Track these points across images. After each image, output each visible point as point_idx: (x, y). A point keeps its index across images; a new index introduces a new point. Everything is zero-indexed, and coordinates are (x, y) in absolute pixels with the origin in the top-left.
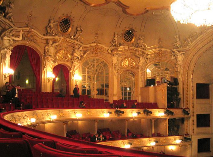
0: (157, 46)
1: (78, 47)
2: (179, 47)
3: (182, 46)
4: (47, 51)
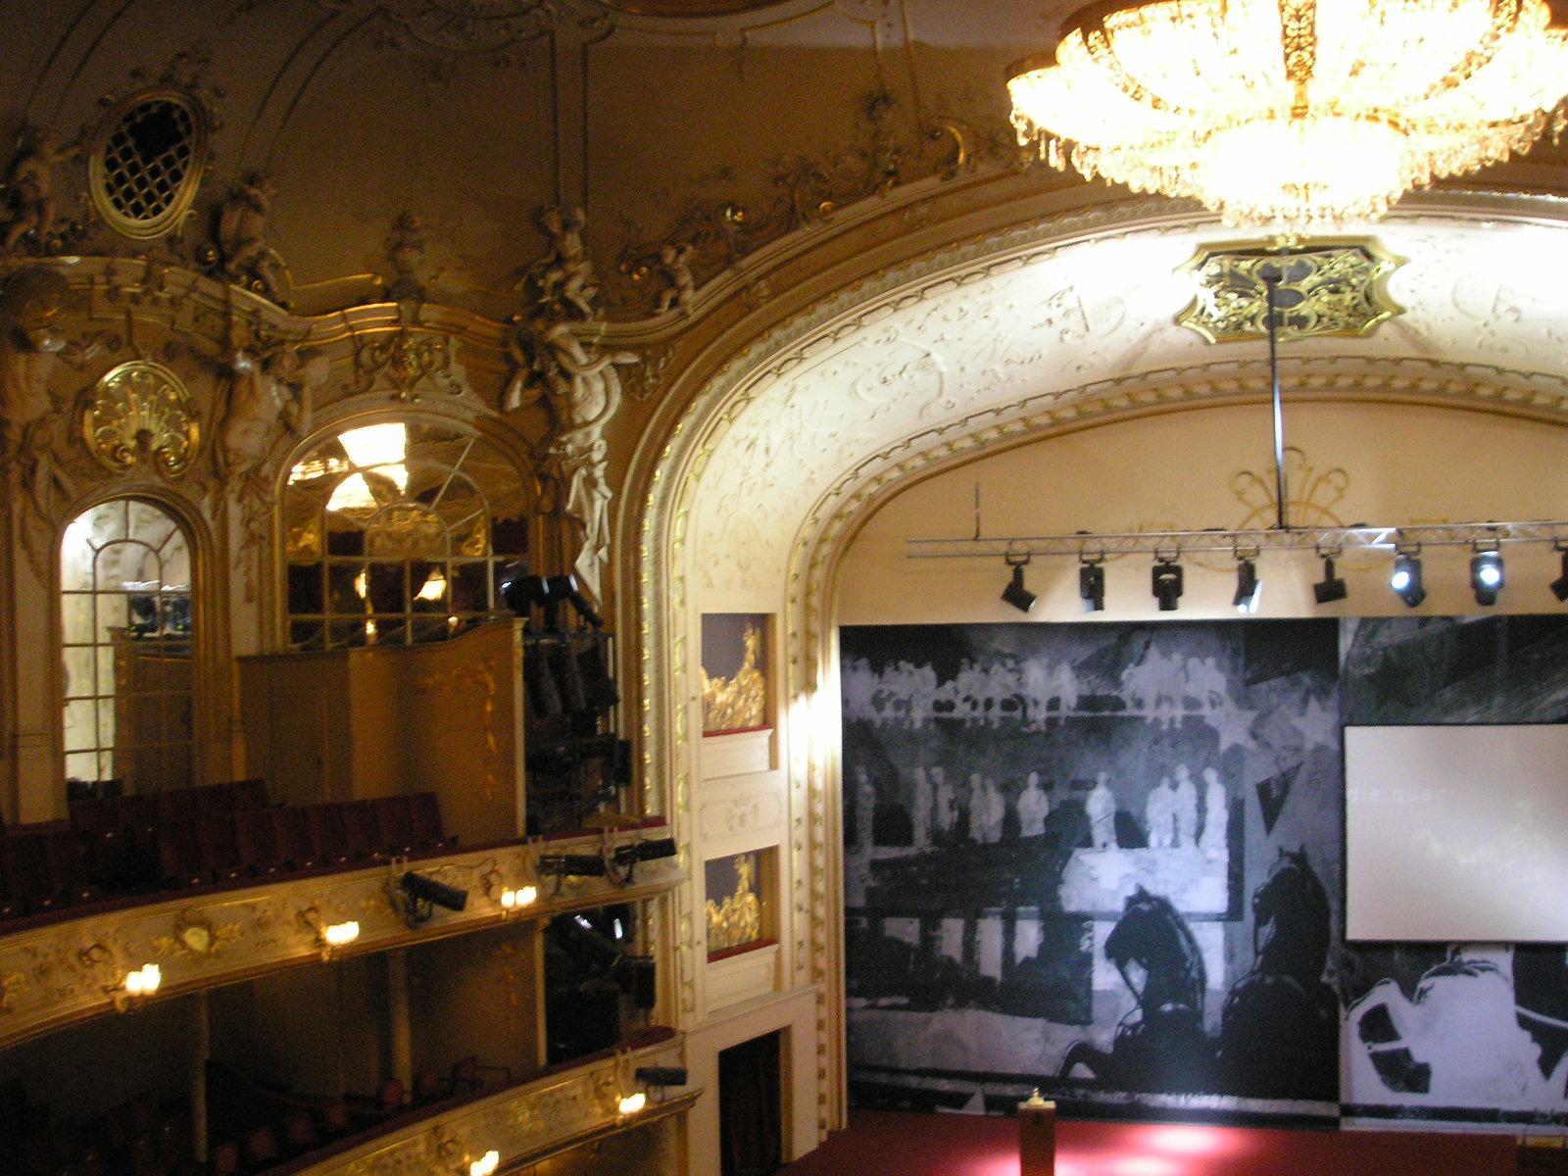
0: (379, 282)
2: (586, 308)
3: (609, 304)
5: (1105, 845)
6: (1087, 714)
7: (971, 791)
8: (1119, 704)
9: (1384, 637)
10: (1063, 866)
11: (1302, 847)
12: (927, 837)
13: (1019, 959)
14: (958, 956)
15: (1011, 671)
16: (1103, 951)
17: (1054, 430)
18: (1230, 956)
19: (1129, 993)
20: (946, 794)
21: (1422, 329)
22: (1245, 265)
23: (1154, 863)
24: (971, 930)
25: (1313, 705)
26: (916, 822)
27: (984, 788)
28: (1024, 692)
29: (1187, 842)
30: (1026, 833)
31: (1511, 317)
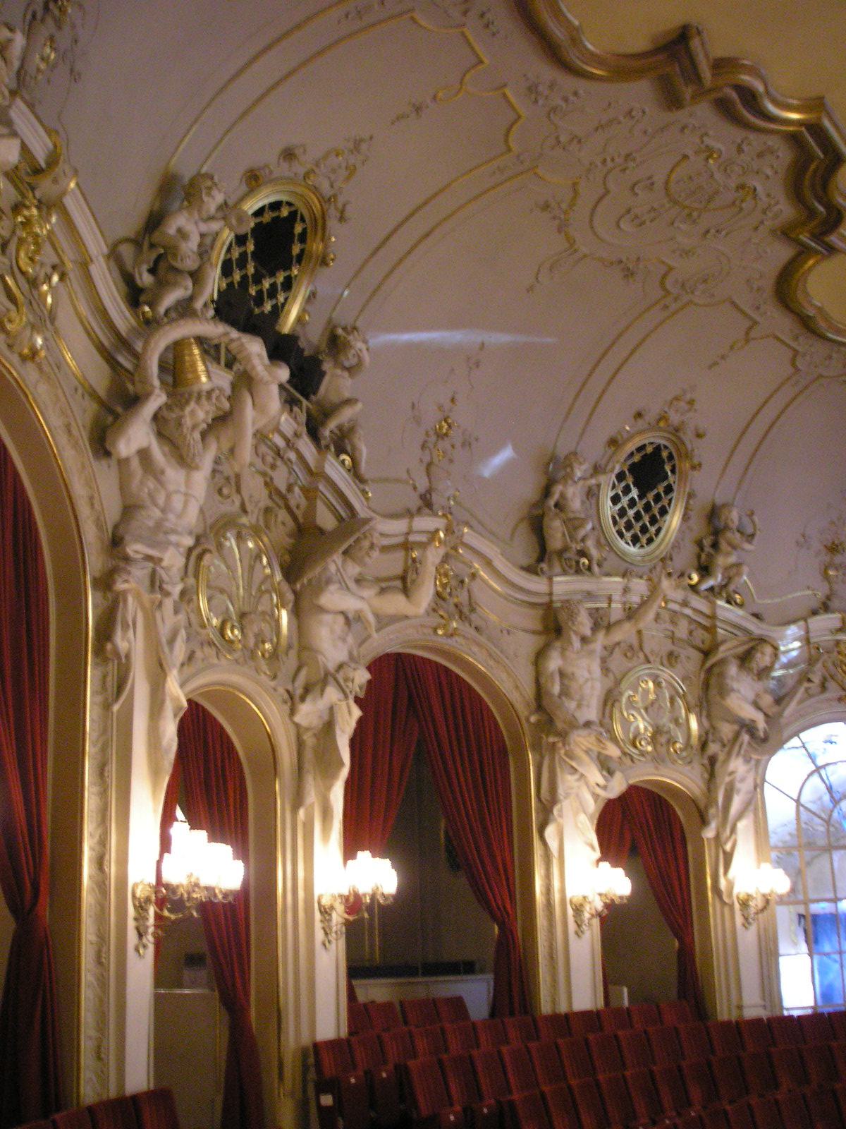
1: (741, 650)
4: (556, 689)
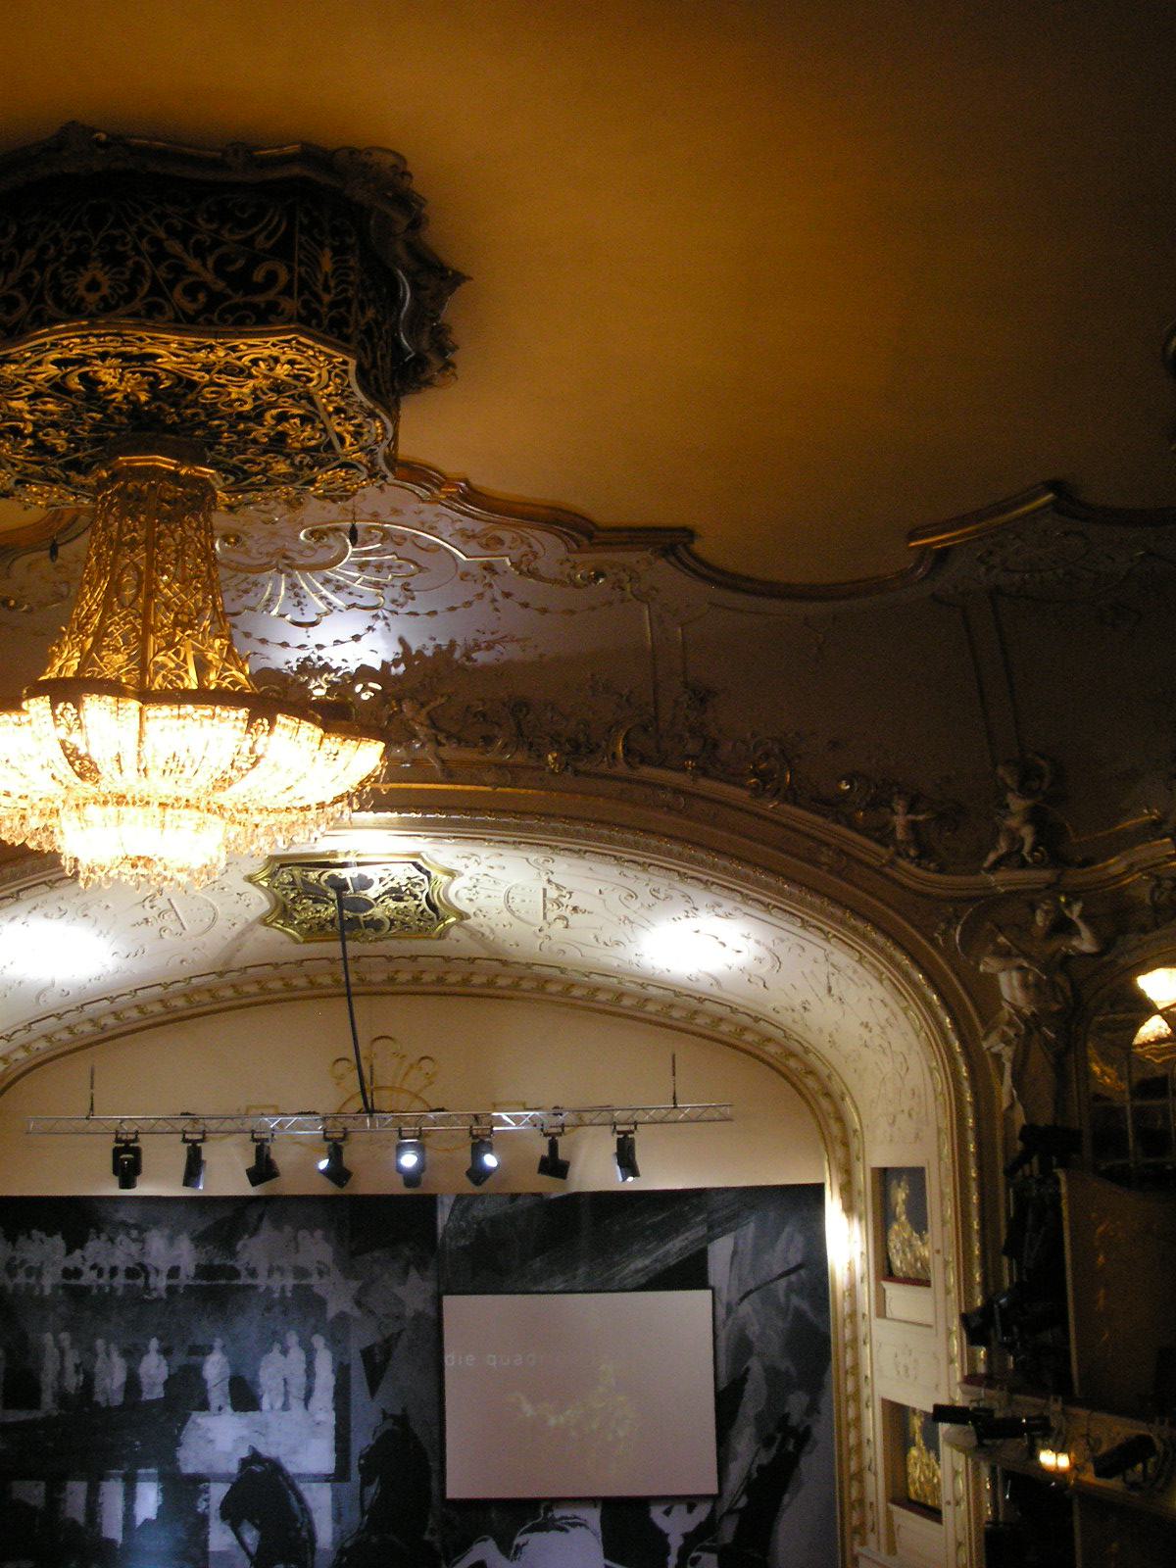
5: (220, 1409)
6: (204, 1282)
7: (96, 1356)
8: (234, 1273)
9: (478, 1211)
10: (180, 1429)
11: (404, 1410)
12: (54, 1401)
13: (139, 1520)
14: (81, 1519)
15: (134, 1240)
16: (218, 1515)
17: (169, 1017)
18: (338, 1516)
19: (243, 1553)
20: (72, 1359)
21: (487, 932)
22: (313, 875)
23: (267, 1426)
24: (93, 1493)
25: (413, 1273)
26: (44, 1388)
27: (108, 1355)
28: (146, 1261)
29: (296, 1404)
30: (146, 1397)
31: (560, 924)
